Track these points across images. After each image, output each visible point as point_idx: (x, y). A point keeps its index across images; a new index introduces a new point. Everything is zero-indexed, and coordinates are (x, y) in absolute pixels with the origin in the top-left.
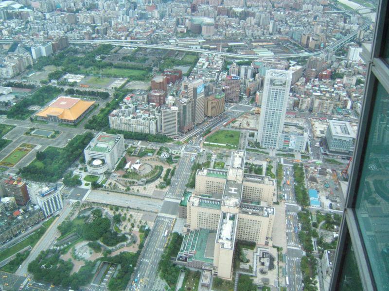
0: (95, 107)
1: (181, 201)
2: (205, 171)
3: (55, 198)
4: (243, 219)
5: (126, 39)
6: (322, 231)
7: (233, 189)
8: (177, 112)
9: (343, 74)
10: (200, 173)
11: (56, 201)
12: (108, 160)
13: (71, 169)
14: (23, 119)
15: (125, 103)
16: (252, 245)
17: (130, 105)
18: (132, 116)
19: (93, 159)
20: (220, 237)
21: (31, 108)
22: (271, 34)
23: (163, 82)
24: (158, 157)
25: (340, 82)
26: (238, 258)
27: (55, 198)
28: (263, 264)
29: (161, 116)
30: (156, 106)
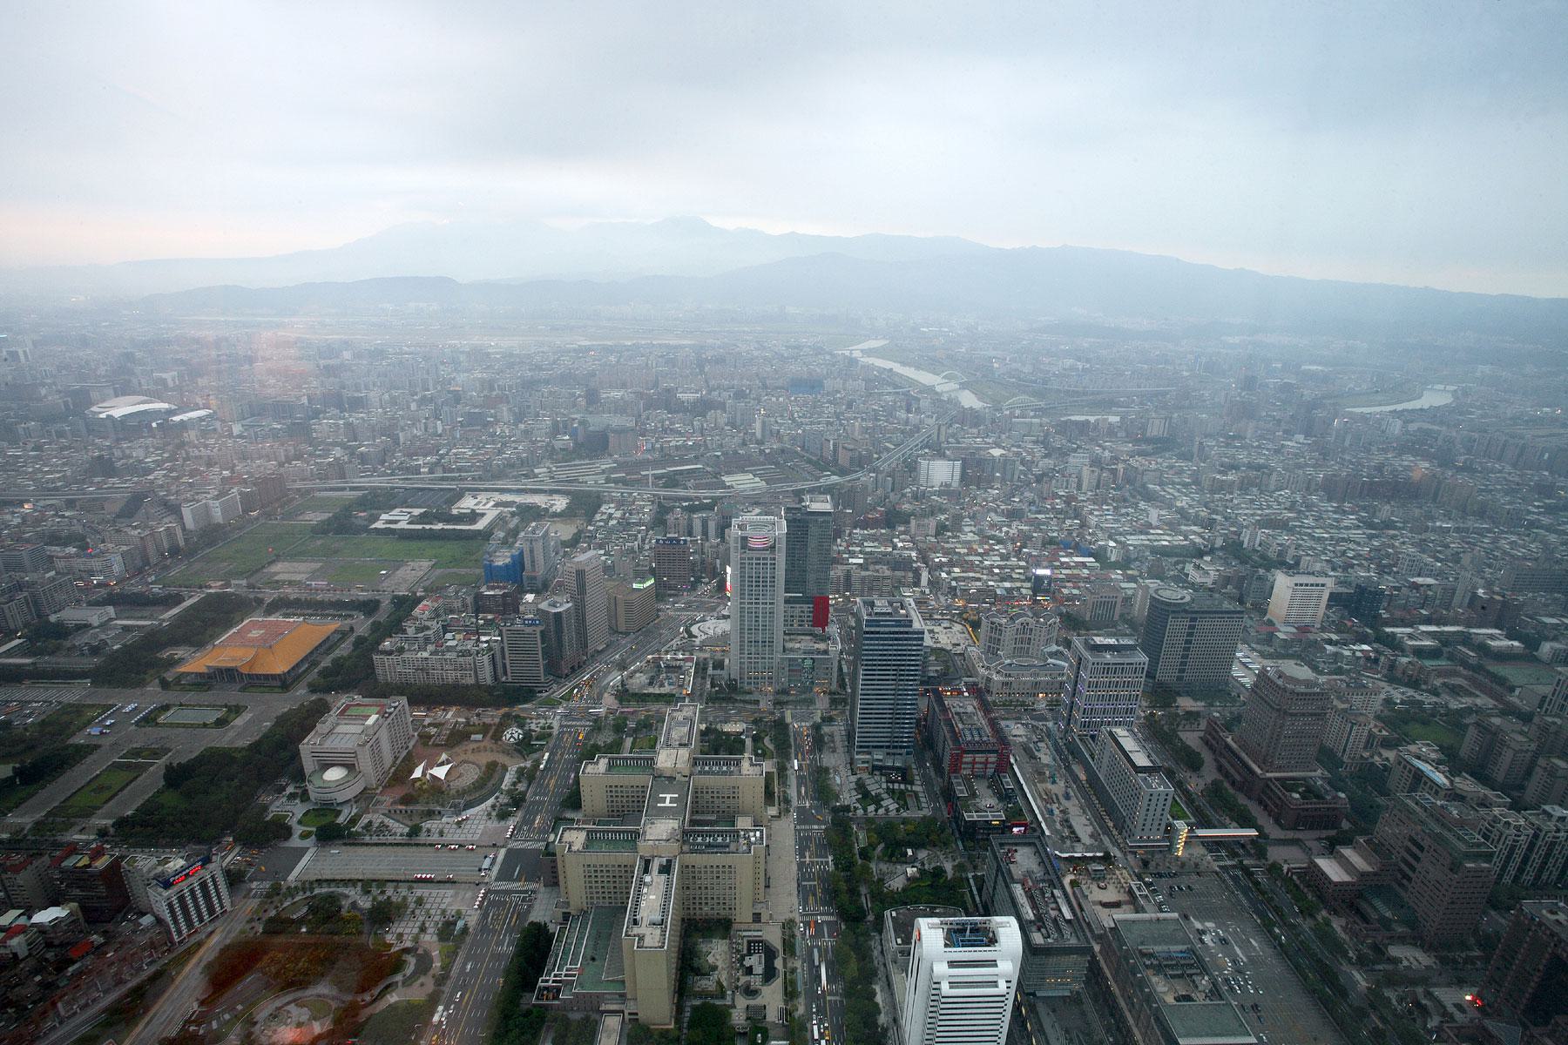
0: (343, 635)
2: (603, 764)
3: (204, 886)
5: (431, 472)
6: (884, 867)
7: (668, 796)
10: (590, 769)
12: (365, 763)
13: (264, 799)
14: (141, 683)
16: (722, 926)
18: (431, 648)
19: (326, 767)
20: (635, 922)
25: (904, 533)
26: (688, 965)
27: (204, 886)
28: (749, 971)
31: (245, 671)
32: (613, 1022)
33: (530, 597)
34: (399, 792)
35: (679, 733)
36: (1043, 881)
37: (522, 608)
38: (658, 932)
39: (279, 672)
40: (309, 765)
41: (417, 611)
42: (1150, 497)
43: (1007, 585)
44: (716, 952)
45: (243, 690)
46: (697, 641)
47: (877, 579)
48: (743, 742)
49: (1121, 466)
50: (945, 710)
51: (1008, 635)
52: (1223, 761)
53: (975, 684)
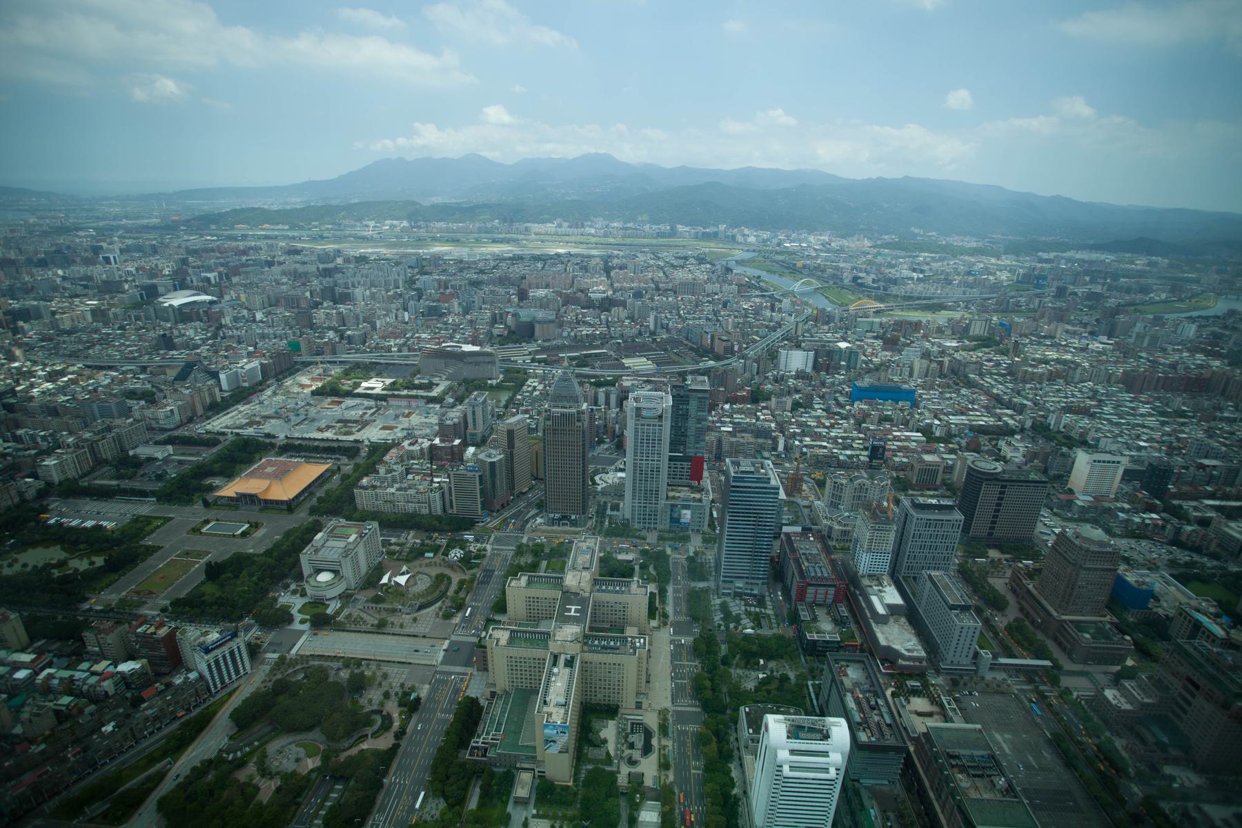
5: (400, 351)
6: (739, 671)
7: (573, 608)
8: (477, 474)
9: (771, 393)
10: (514, 583)
12: (347, 570)
14: (190, 502)
16: (611, 711)
17: (395, 467)
18: (396, 486)
20: (545, 702)
21: (208, 481)
22: (653, 333)
26: (585, 736)
28: (632, 746)
32: (526, 777)
34: (371, 593)
35: (583, 559)
36: (869, 691)
38: (562, 711)
39: (285, 498)
40: (307, 570)
41: (386, 458)
42: (970, 384)
43: (848, 452)
44: (609, 731)
45: (262, 510)
46: (599, 488)
47: (743, 444)
48: (633, 569)
49: (946, 359)
50: (794, 550)
51: (847, 494)
52: (1024, 603)
53: (819, 531)
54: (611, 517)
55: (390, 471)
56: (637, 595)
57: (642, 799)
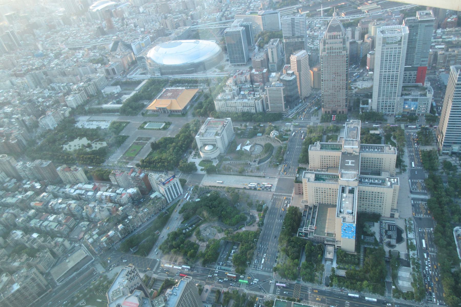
1: (296, 178)
3: (174, 185)
4: (364, 192)
7: (350, 161)
8: (282, 88)
10: (313, 148)
11: (175, 188)
12: (219, 144)
14: (136, 114)
15: (229, 86)
18: (236, 98)
19: (205, 145)
20: (340, 211)
21: (141, 102)
23: (264, 59)
24: (268, 137)
26: (361, 230)
27: (174, 185)
29: (266, 94)
30: (259, 85)
31: (168, 109)
33: (273, 74)
37: (270, 79)
39: (180, 109)
40: (199, 146)
44: (375, 228)
45: (169, 116)
54: (363, 109)
55: (231, 91)
56: (388, 155)
57: (399, 265)
